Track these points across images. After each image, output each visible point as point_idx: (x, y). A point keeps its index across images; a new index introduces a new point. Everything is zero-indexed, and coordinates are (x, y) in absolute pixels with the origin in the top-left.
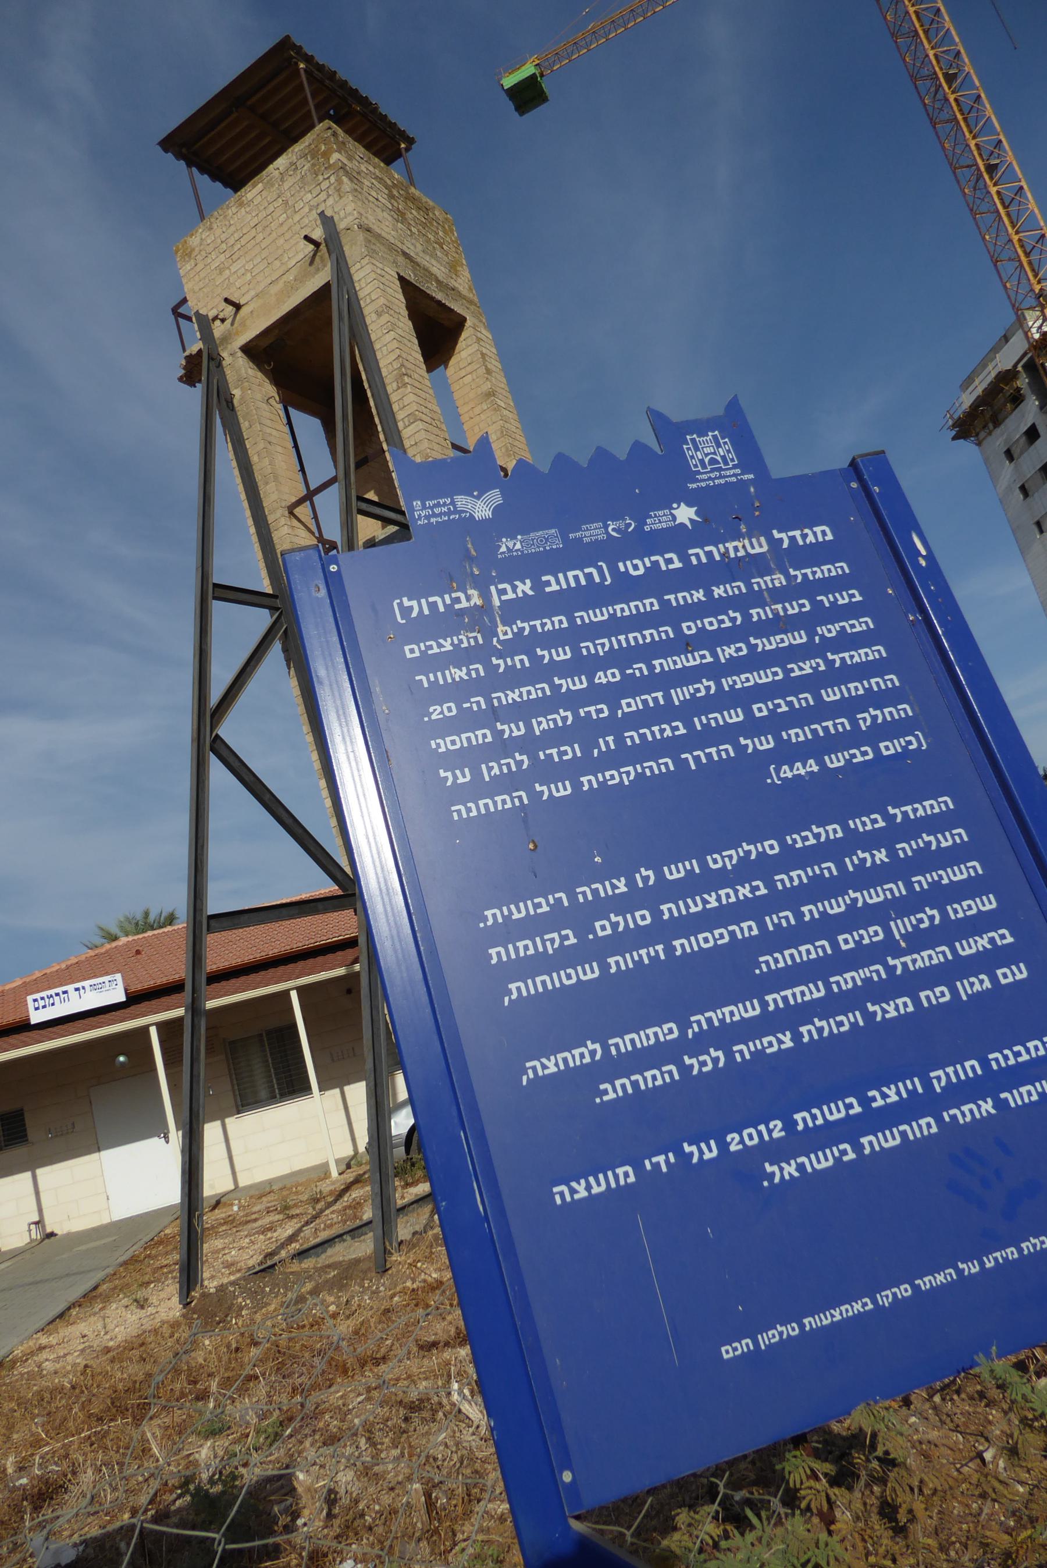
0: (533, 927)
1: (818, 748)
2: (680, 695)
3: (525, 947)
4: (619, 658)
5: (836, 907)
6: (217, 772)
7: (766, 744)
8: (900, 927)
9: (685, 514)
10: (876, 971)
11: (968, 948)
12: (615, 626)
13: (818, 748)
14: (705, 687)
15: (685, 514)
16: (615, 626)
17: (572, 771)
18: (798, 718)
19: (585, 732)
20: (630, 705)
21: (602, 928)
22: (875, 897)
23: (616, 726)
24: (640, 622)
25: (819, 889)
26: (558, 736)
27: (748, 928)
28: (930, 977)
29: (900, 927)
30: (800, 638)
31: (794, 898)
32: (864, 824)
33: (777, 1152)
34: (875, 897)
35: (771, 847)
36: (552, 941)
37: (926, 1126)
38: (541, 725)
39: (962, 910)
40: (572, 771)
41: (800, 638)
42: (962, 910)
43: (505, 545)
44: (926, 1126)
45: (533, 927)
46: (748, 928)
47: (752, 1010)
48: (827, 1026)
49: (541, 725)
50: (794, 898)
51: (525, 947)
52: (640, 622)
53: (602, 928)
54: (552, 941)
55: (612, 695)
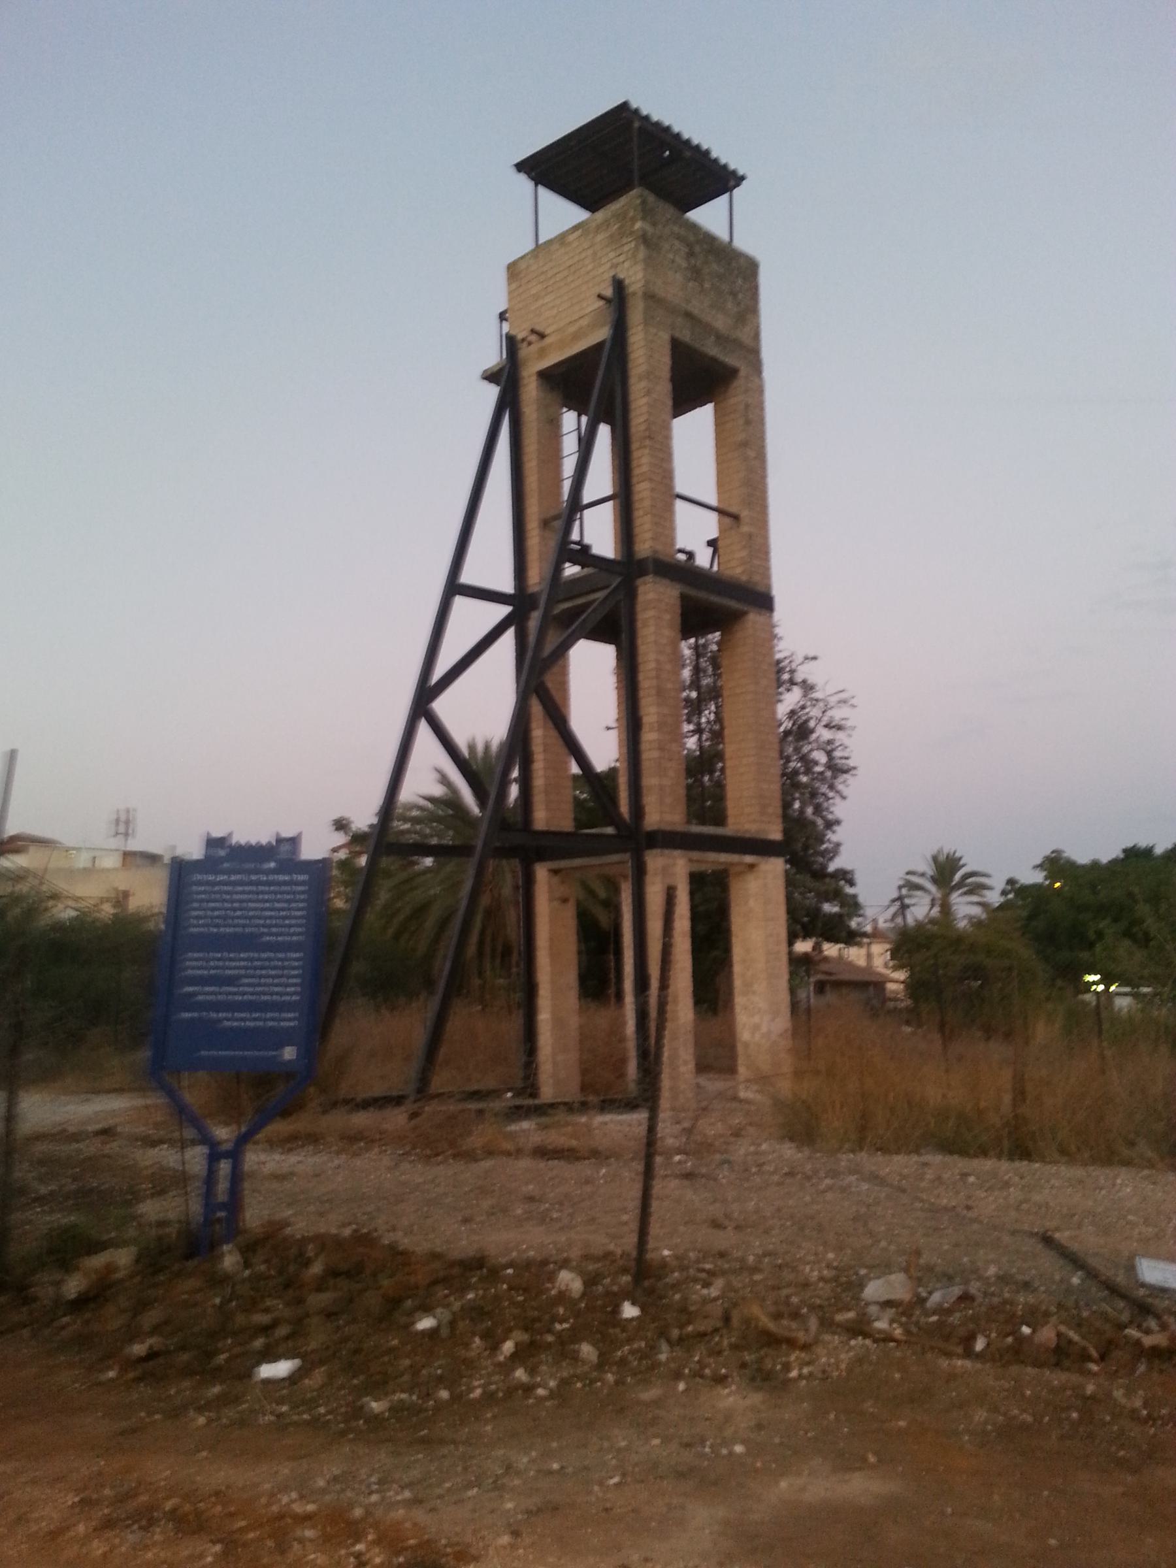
0: (197, 960)
1: (277, 935)
2: (251, 913)
3: (195, 963)
4: (241, 901)
5: (264, 972)
6: (423, 728)
7: (266, 930)
8: (276, 981)
9: (272, 865)
10: (266, 989)
11: (288, 989)
12: (243, 892)
13: (277, 935)
14: (257, 913)
15: (272, 865)
16: (243, 892)
17: (217, 926)
18: (276, 926)
19: (225, 918)
20: (239, 913)
21: (212, 964)
22: (273, 972)
23: (233, 918)
24: (250, 893)
25: (262, 968)
26: (218, 917)
27: (243, 972)
28: (277, 994)
29: (276, 981)
30: (286, 905)
31: (255, 968)
32: (280, 955)
33: (228, 1020)
34: (273, 972)
35: (256, 955)
36: (200, 963)
37: (261, 1024)
38: (216, 913)
39: (291, 981)
40: (217, 926)
41: (286, 905)
42: (291, 981)
43: (226, 865)
44: (261, 1024)
45: (197, 960)
46: (243, 972)
47: (235, 989)
48: (250, 997)
49: (216, 913)
50: (255, 968)
51: (195, 963)
52: (250, 893)
53: (212, 964)
54: (200, 963)
55: (235, 910)
